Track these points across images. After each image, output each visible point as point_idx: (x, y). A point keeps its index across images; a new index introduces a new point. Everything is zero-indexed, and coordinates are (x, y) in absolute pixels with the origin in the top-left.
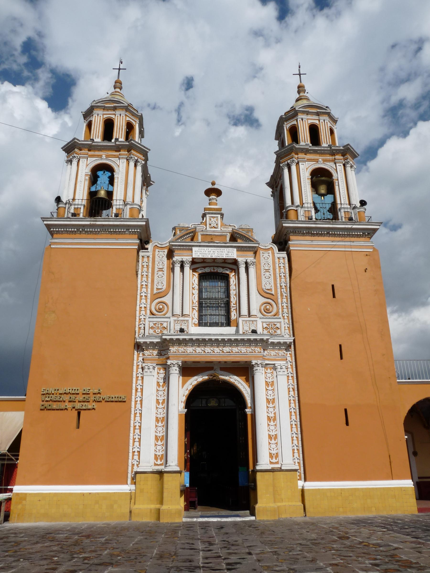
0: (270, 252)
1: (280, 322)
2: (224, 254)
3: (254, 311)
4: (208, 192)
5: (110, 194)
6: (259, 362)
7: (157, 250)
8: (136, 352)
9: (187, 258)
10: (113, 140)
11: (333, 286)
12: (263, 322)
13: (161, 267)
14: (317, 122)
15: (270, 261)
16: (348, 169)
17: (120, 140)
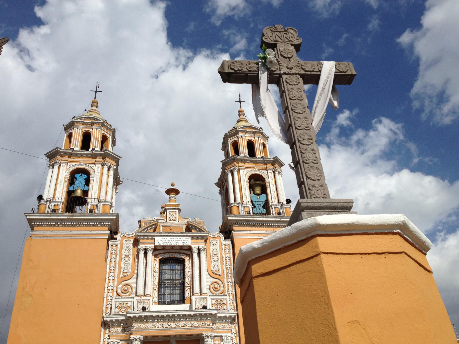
0: (218, 240)
1: (226, 299)
2: (181, 242)
3: (204, 290)
4: (169, 192)
5: (86, 193)
6: (209, 334)
7: (125, 240)
8: (102, 329)
9: (150, 246)
10: (90, 150)
12: (212, 299)
13: (127, 254)
14: (253, 139)
15: (218, 247)
16: (277, 175)
17: (96, 149)
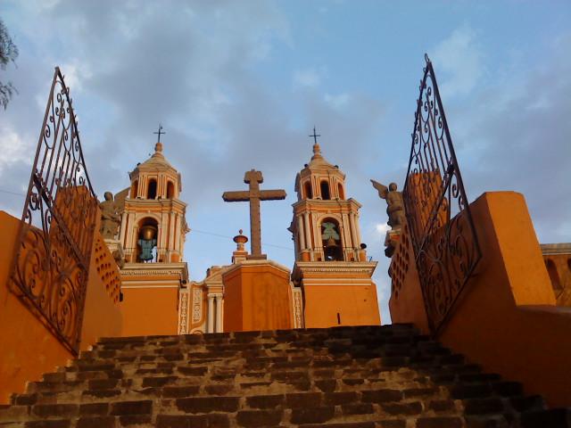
4: (236, 239)
10: (157, 197)
11: (338, 314)
14: (327, 179)
